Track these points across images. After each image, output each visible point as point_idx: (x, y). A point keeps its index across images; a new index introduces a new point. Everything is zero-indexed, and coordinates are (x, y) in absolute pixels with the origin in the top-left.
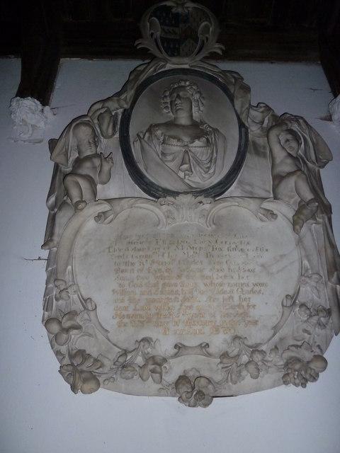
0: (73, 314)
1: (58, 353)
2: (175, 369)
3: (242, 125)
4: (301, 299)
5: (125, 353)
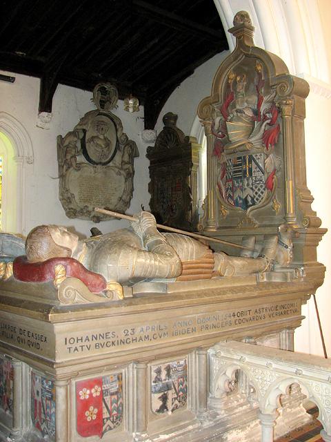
0: (69, 198)
1: (65, 208)
2: (93, 214)
3: (117, 141)
4: (123, 198)
5: (82, 209)
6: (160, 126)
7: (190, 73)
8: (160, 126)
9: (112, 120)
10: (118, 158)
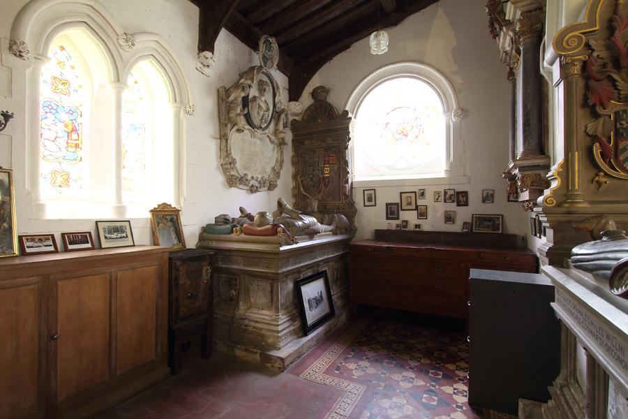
6: (306, 100)
7: (347, 47)
8: (306, 100)
9: (272, 82)
10: (272, 126)
